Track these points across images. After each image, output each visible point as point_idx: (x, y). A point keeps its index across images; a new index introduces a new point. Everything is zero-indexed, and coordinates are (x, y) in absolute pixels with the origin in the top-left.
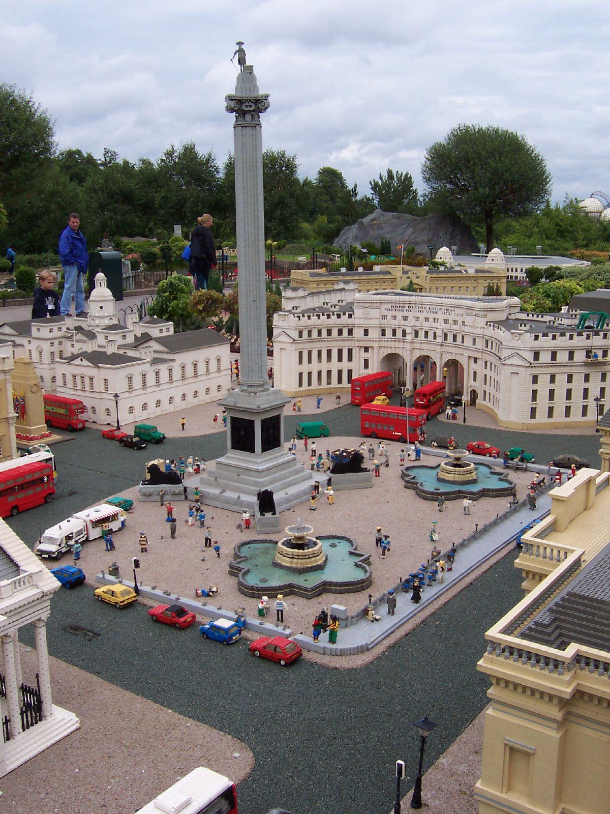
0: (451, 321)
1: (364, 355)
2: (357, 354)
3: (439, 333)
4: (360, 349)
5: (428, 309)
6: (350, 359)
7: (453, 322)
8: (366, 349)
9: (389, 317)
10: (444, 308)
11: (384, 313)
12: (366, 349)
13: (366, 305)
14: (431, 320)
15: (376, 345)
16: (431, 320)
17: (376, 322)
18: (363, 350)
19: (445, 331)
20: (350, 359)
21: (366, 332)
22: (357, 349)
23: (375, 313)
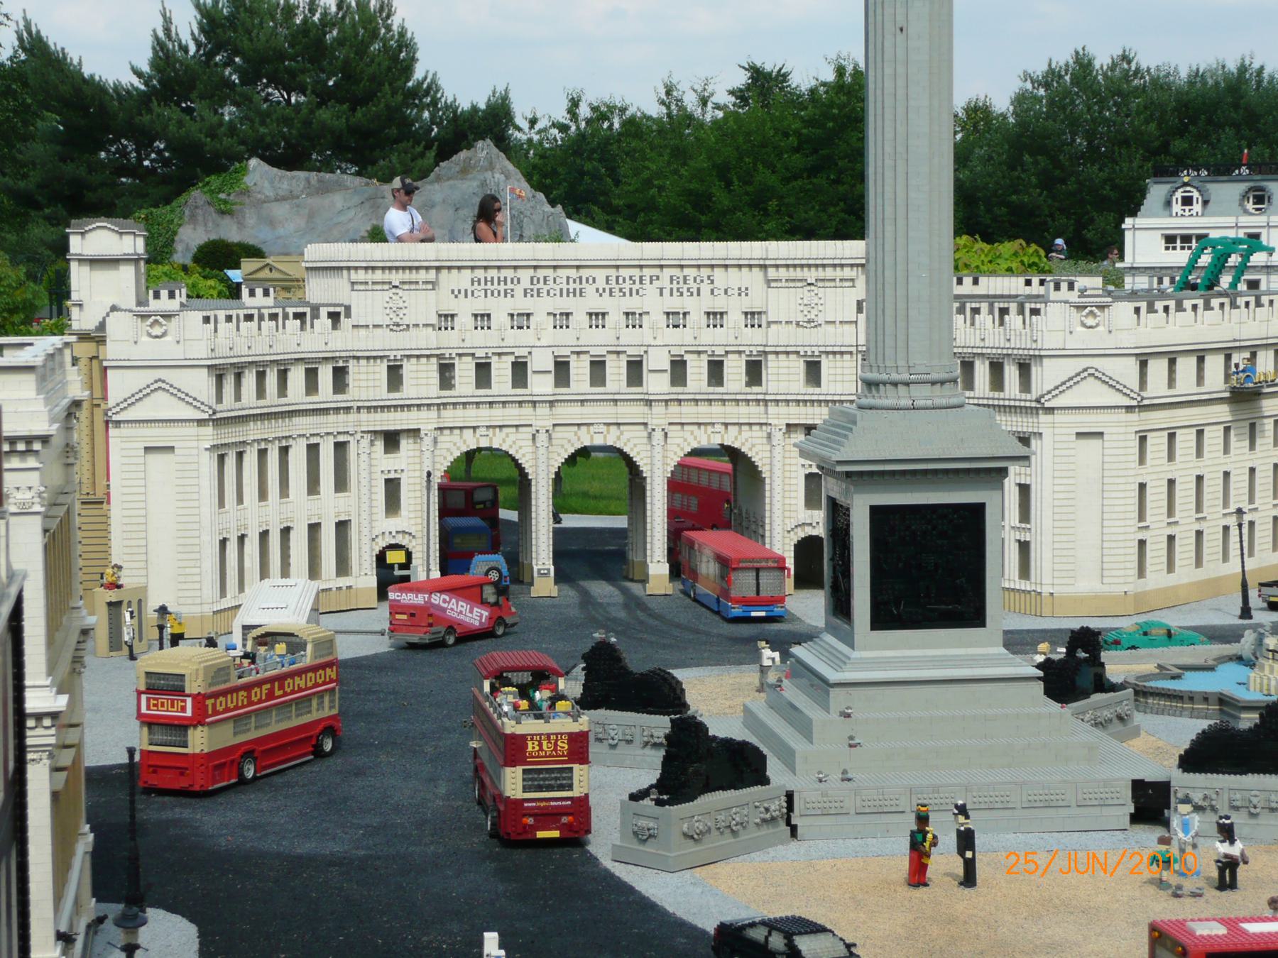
0: (697, 318)
1: (387, 463)
2: (364, 457)
3: (542, 361)
4: (372, 443)
5: (601, 283)
6: (341, 483)
7: (470, 321)
8: (391, 440)
9: (464, 320)
10: (668, 273)
11: (450, 305)
12: (391, 440)
13: (396, 278)
14: (615, 318)
15: (425, 421)
16: (615, 318)
17: (427, 339)
18: (380, 445)
19: (675, 351)
20: (341, 483)
21: (395, 376)
22: (365, 442)
23: (422, 306)
